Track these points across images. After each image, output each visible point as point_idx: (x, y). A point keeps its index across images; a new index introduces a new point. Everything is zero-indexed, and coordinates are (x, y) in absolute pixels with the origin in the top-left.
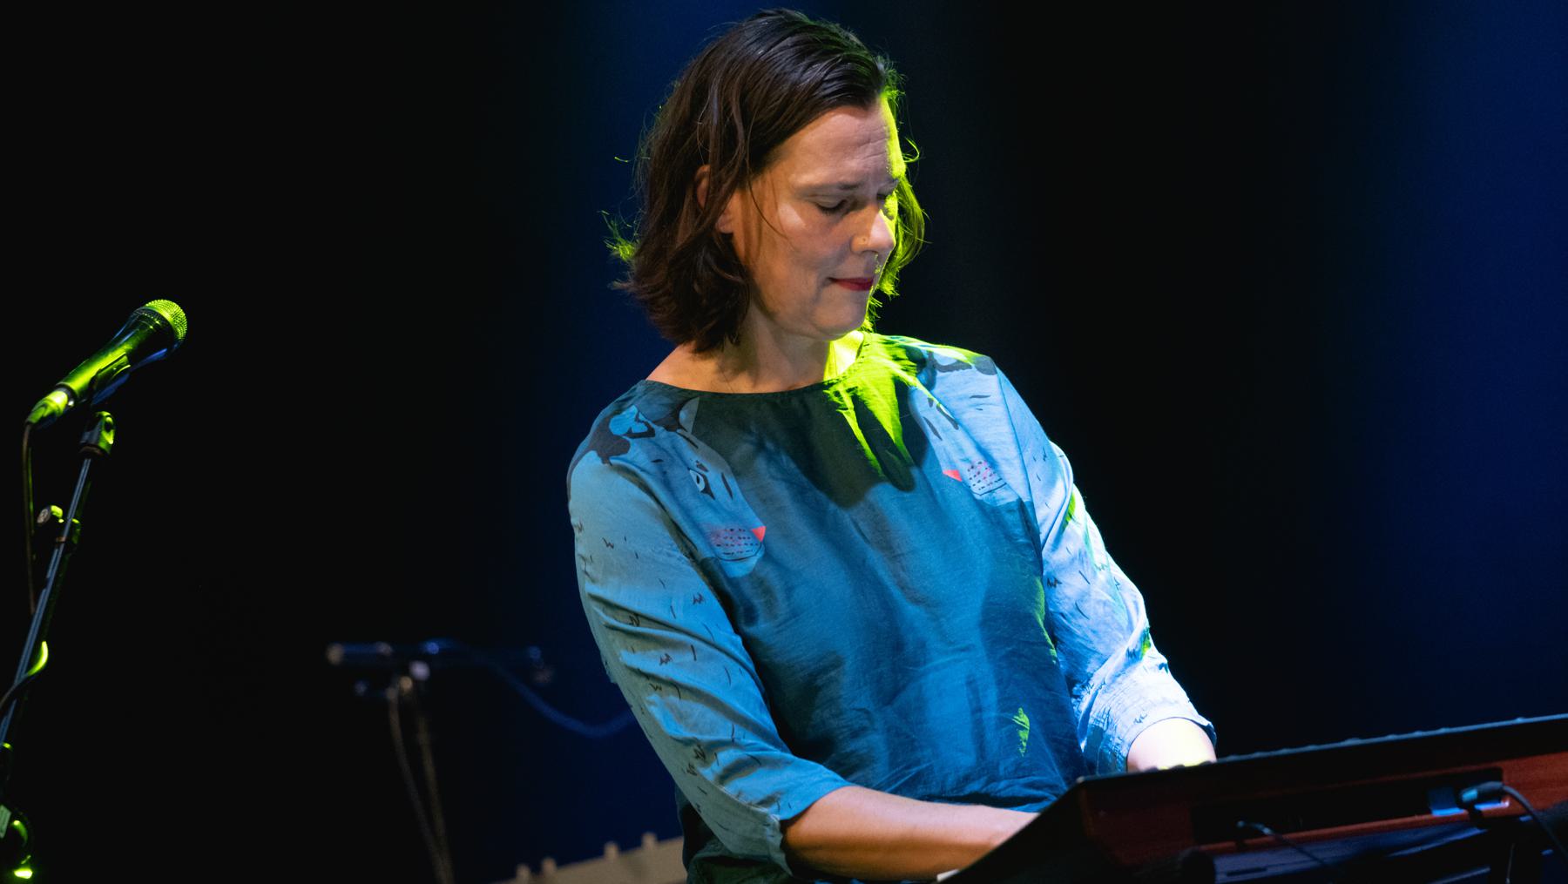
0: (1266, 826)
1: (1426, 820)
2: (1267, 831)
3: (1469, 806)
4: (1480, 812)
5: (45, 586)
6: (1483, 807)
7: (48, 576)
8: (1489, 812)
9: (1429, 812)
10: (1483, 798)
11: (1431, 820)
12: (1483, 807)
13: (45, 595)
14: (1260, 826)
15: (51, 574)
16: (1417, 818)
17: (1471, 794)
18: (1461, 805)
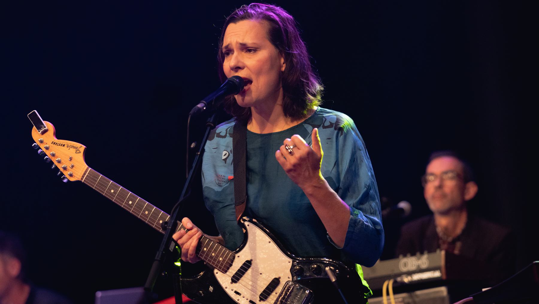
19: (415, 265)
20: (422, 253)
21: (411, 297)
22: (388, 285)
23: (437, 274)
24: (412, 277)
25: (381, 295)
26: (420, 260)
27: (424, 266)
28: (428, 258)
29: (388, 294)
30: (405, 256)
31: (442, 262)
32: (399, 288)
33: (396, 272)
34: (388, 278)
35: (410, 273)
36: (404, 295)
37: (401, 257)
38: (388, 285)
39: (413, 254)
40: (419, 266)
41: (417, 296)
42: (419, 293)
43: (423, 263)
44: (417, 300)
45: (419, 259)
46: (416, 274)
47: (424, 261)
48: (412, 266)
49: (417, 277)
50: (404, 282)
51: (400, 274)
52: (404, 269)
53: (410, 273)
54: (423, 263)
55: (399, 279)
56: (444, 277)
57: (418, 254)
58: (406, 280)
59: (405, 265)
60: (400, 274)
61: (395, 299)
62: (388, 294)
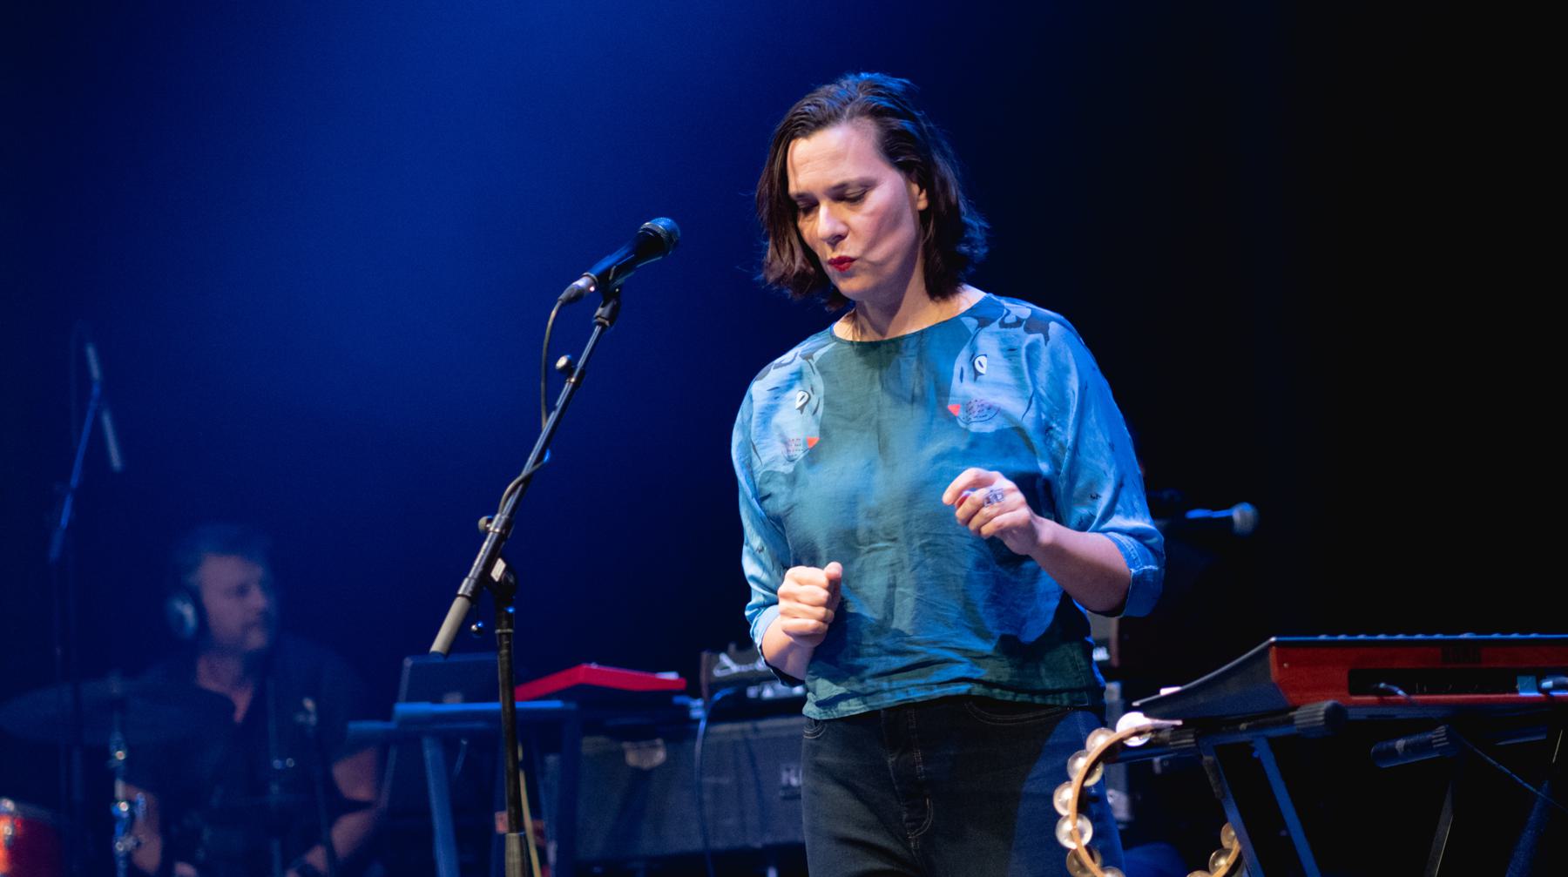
0: (1401, 688)
1: (1513, 698)
2: (1400, 692)
3: (1546, 691)
4: (1552, 696)
5: (555, 408)
6: (1555, 694)
7: (558, 403)
8: (1560, 698)
9: (1516, 692)
10: (1557, 687)
11: (1517, 698)
12: (1555, 694)
13: (554, 416)
14: (1396, 689)
15: (560, 403)
16: (1507, 695)
17: (1548, 684)
18: (1540, 690)
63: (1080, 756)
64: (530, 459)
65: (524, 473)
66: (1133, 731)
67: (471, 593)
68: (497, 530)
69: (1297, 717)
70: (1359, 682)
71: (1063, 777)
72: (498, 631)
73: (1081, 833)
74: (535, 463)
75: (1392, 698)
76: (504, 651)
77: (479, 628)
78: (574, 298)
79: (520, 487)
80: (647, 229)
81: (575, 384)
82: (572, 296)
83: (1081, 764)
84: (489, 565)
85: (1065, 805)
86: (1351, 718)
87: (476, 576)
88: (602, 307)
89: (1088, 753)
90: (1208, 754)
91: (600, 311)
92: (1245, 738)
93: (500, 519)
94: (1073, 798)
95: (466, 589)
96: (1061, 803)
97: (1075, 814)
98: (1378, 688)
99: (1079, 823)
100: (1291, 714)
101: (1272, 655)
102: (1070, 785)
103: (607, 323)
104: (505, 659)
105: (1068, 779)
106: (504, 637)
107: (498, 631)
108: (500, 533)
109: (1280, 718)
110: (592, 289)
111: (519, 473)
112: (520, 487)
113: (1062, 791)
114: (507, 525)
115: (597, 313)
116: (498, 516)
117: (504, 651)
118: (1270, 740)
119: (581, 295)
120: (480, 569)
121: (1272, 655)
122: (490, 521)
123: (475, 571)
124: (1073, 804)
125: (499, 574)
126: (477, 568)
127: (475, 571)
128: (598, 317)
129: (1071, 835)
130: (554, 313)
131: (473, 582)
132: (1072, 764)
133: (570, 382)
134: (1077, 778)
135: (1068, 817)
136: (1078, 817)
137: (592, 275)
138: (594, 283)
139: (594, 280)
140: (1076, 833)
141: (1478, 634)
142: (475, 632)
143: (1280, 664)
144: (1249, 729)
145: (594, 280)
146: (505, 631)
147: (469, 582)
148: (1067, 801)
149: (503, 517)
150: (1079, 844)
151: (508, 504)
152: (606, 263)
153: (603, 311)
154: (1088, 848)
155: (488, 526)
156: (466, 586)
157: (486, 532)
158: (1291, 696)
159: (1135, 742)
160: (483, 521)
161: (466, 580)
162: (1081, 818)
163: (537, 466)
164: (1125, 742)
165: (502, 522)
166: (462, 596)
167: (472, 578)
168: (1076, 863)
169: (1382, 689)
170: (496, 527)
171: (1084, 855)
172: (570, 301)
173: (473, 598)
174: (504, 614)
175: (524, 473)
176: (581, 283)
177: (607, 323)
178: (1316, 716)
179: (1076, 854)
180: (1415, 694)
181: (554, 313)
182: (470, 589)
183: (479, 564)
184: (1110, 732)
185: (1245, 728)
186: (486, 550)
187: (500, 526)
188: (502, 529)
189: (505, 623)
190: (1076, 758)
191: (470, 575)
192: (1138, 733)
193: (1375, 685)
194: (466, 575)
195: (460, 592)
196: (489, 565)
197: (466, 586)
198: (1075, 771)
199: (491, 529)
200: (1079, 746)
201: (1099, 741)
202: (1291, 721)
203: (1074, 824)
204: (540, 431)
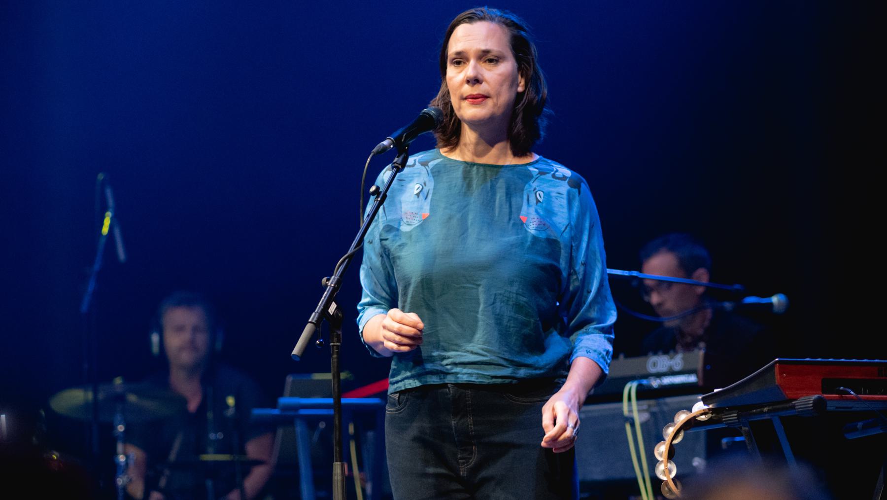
2: (852, 393)
19: (666, 366)
20: (676, 352)
21: (658, 405)
22: (631, 387)
23: (692, 379)
24: (661, 381)
25: (620, 399)
26: (673, 360)
27: (677, 368)
28: (683, 359)
29: (629, 399)
30: (655, 353)
31: (700, 365)
32: (644, 394)
33: (643, 372)
34: (632, 379)
35: (659, 375)
36: (652, 402)
37: (650, 354)
38: (631, 387)
39: (666, 352)
40: (671, 368)
41: (666, 404)
42: (669, 400)
43: (676, 364)
44: (665, 408)
45: (672, 358)
46: (666, 377)
47: (677, 361)
48: (663, 366)
49: (667, 381)
50: (652, 385)
51: (647, 376)
52: (653, 370)
53: (659, 375)
54: (676, 364)
55: (645, 382)
56: (701, 383)
57: (672, 353)
58: (655, 383)
59: (655, 364)
60: (647, 376)
61: (638, 405)
62: (629, 399)
63: (670, 426)
64: (353, 244)
65: (349, 252)
66: (703, 412)
67: (316, 321)
68: (332, 285)
69: (796, 404)
70: (828, 386)
71: (660, 439)
72: (332, 344)
73: (670, 471)
74: (356, 247)
75: (847, 396)
76: (335, 356)
77: (320, 342)
78: (380, 151)
79: (347, 260)
80: (425, 113)
81: (379, 201)
82: (380, 150)
83: (671, 431)
84: (327, 305)
85: (661, 455)
86: (828, 408)
87: (319, 312)
88: (397, 157)
89: (676, 424)
90: (744, 426)
91: (396, 159)
92: (767, 417)
93: (334, 279)
94: (665, 450)
95: (313, 319)
96: (659, 453)
97: (666, 460)
98: (839, 390)
99: (669, 465)
100: (794, 402)
101: (777, 369)
102: (664, 444)
103: (400, 167)
104: (335, 360)
105: (664, 440)
106: (335, 347)
107: (332, 344)
108: (334, 287)
109: (788, 405)
110: (392, 146)
111: (347, 253)
112: (347, 260)
113: (660, 446)
114: (338, 282)
115: (395, 161)
116: (333, 277)
117: (335, 356)
118: (781, 418)
119: (385, 149)
120: (322, 307)
121: (777, 369)
122: (328, 280)
123: (319, 308)
124: (665, 454)
125: (333, 311)
126: (320, 306)
127: (319, 308)
128: (394, 163)
129: (664, 472)
130: (369, 160)
131: (317, 314)
132: (666, 431)
133: (377, 200)
134: (668, 439)
135: (662, 461)
136: (668, 462)
137: (392, 138)
138: (393, 143)
139: (393, 141)
140: (667, 471)
141: (869, 360)
142: (318, 344)
143: (781, 374)
144: (769, 411)
145: (393, 141)
146: (335, 344)
147: (315, 315)
148: (663, 452)
149: (336, 278)
150: (668, 477)
151: (339, 270)
152: (399, 132)
153: (398, 160)
154: (673, 479)
155: (327, 282)
156: (313, 317)
157: (326, 286)
158: (787, 393)
159: (703, 418)
160: (324, 279)
161: (314, 314)
162: (670, 463)
163: (357, 248)
164: (697, 418)
165: (336, 280)
166: (311, 322)
167: (317, 312)
168: (666, 489)
169: (842, 390)
170: (332, 283)
171: (671, 484)
172: (378, 153)
173: (317, 324)
174: (335, 334)
175: (349, 252)
176: (385, 143)
177: (400, 167)
178: (809, 404)
179: (666, 482)
180: (861, 394)
181: (369, 160)
182: (315, 319)
183: (321, 304)
184: (688, 412)
185: (767, 410)
186: (325, 297)
187: (334, 283)
188: (335, 285)
189: (335, 339)
190: (668, 427)
191: (316, 311)
192: (704, 413)
193: (837, 388)
194: (314, 311)
195: (310, 321)
196: (327, 305)
197: (313, 317)
198: (667, 435)
199: (329, 284)
200: (670, 420)
201: (682, 418)
202: (793, 407)
203: (666, 466)
204: (360, 228)
